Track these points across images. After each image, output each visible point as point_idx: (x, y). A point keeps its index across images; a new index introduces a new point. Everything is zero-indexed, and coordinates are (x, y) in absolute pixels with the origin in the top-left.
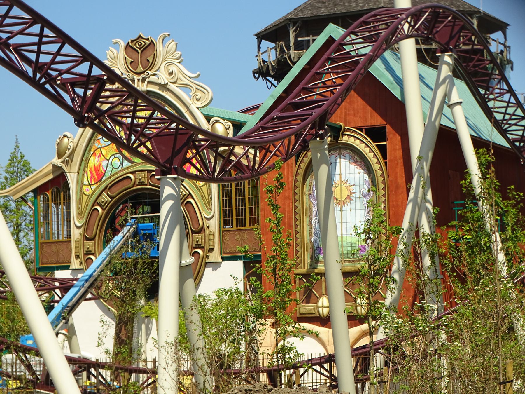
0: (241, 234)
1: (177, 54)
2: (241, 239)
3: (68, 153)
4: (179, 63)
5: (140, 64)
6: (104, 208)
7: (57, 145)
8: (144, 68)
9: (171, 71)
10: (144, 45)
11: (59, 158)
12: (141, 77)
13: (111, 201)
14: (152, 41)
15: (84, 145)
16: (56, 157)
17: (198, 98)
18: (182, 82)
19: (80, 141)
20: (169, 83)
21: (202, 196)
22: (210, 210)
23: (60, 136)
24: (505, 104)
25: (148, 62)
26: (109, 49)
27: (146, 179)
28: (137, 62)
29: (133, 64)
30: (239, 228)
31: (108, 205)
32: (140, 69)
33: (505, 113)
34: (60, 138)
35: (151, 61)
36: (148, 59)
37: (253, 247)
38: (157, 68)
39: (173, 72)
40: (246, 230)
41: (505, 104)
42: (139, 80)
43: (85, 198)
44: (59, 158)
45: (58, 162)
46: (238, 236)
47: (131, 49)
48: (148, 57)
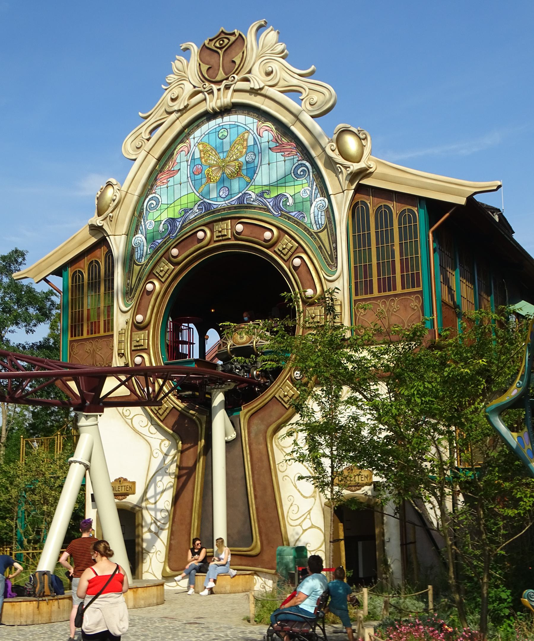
0: (388, 303)
1: (280, 47)
2: (388, 310)
3: (113, 205)
4: (283, 58)
5: (221, 68)
6: (163, 280)
7: (98, 198)
8: (226, 74)
9: (270, 69)
10: (228, 43)
11: (99, 216)
12: (222, 86)
13: (174, 270)
14: (240, 35)
15: (137, 192)
16: (96, 214)
17: (313, 102)
18: (286, 84)
19: (130, 189)
20: (266, 87)
21: (320, 247)
22: (334, 268)
23: (101, 187)
25: (233, 64)
26: (174, 59)
27: (230, 231)
28: (217, 68)
29: (211, 71)
30: (383, 294)
31: (169, 275)
32: (221, 75)
34: (102, 189)
35: (238, 62)
36: (234, 59)
37: (408, 322)
38: (248, 70)
39: (272, 72)
40: (395, 296)
42: (219, 90)
43: (137, 268)
44: (99, 216)
45: (98, 221)
46: (382, 307)
47: (208, 51)
48: (234, 58)
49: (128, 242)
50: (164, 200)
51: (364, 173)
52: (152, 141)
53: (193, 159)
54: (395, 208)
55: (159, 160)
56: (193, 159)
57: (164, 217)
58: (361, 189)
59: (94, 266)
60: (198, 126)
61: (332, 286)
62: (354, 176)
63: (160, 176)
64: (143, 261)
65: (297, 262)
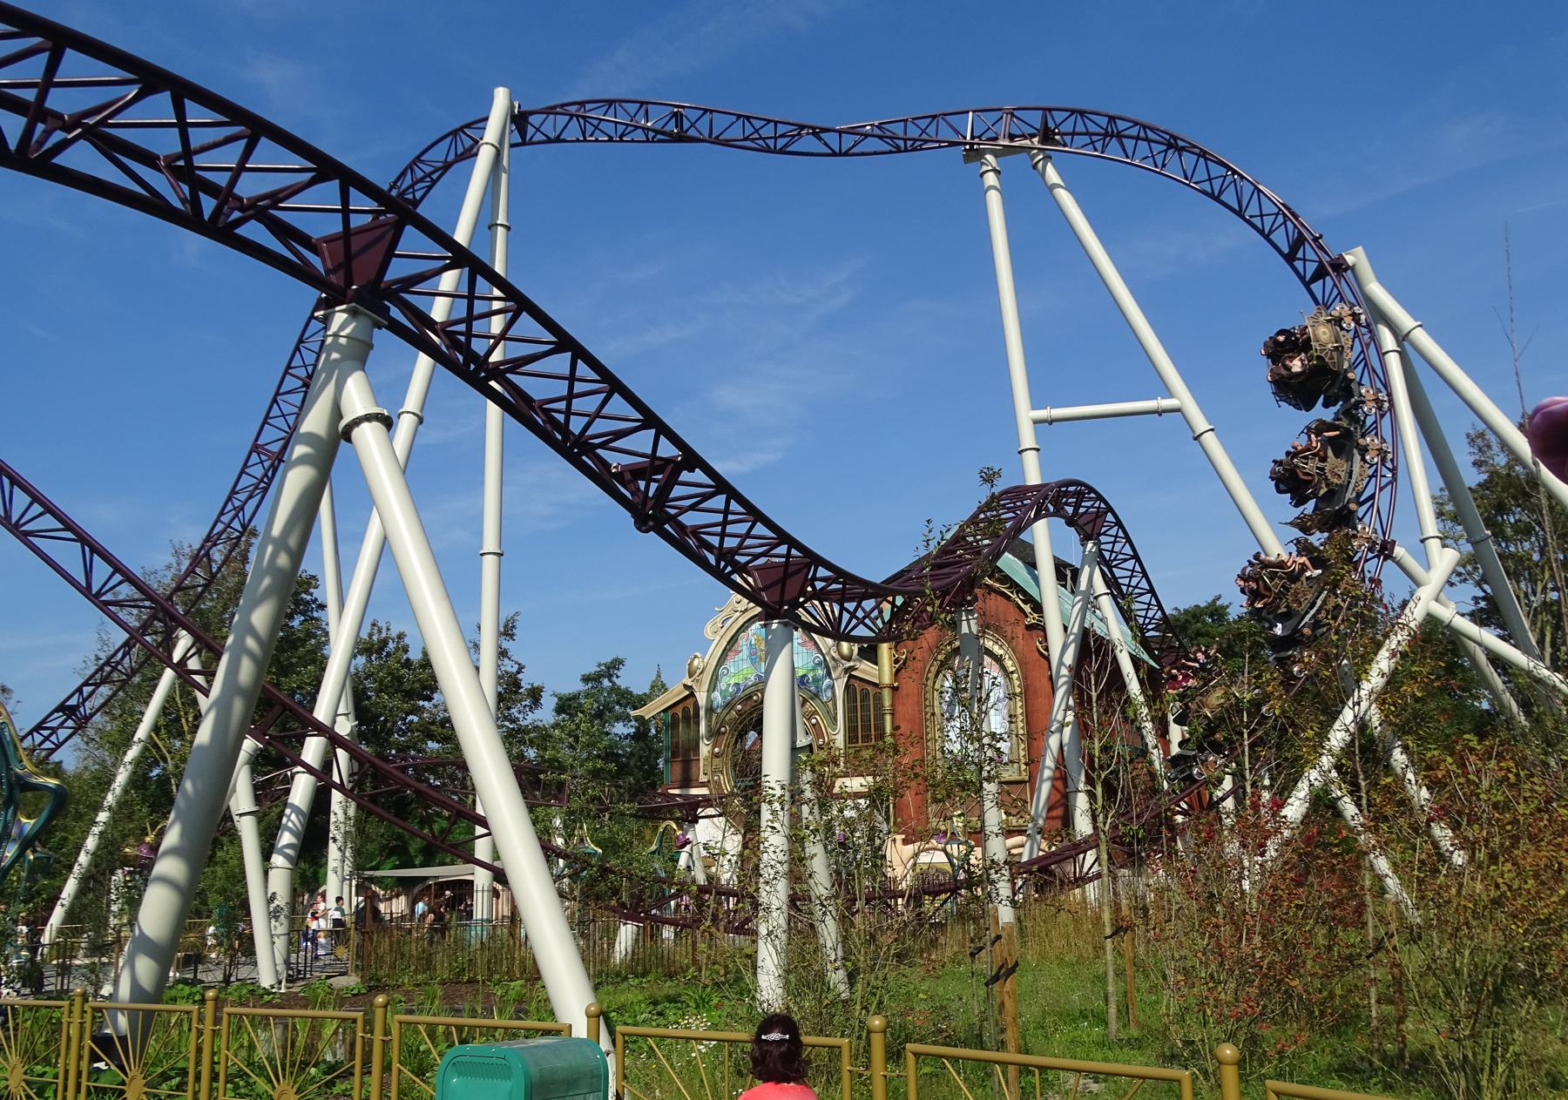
3: (699, 672)
15: (714, 664)
24: (1146, 606)
33: (1145, 617)
41: (1146, 606)
45: (689, 682)
49: (709, 697)
50: (732, 670)
51: (853, 668)
52: (725, 629)
53: (751, 645)
54: (870, 688)
55: (729, 642)
56: (751, 645)
57: (732, 682)
58: (851, 677)
59: (686, 710)
60: (754, 623)
61: (834, 737)
62: (847, 670)
63: (730, 654)
64: (719, 711)
65: (814, 721)
